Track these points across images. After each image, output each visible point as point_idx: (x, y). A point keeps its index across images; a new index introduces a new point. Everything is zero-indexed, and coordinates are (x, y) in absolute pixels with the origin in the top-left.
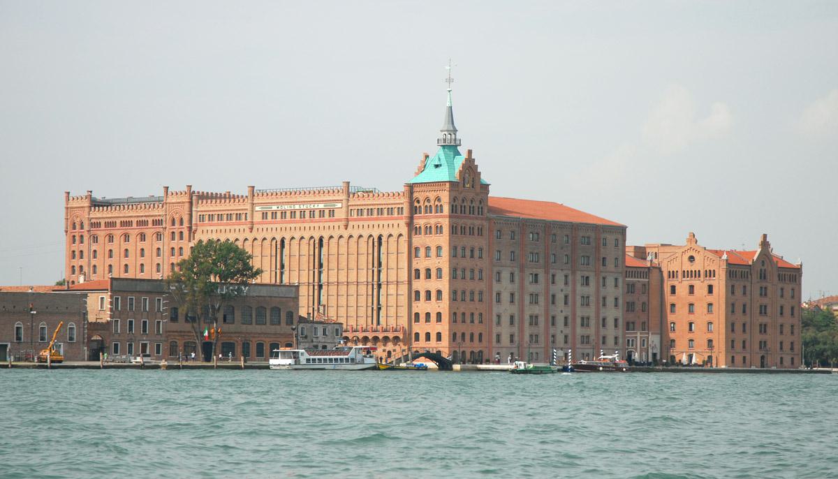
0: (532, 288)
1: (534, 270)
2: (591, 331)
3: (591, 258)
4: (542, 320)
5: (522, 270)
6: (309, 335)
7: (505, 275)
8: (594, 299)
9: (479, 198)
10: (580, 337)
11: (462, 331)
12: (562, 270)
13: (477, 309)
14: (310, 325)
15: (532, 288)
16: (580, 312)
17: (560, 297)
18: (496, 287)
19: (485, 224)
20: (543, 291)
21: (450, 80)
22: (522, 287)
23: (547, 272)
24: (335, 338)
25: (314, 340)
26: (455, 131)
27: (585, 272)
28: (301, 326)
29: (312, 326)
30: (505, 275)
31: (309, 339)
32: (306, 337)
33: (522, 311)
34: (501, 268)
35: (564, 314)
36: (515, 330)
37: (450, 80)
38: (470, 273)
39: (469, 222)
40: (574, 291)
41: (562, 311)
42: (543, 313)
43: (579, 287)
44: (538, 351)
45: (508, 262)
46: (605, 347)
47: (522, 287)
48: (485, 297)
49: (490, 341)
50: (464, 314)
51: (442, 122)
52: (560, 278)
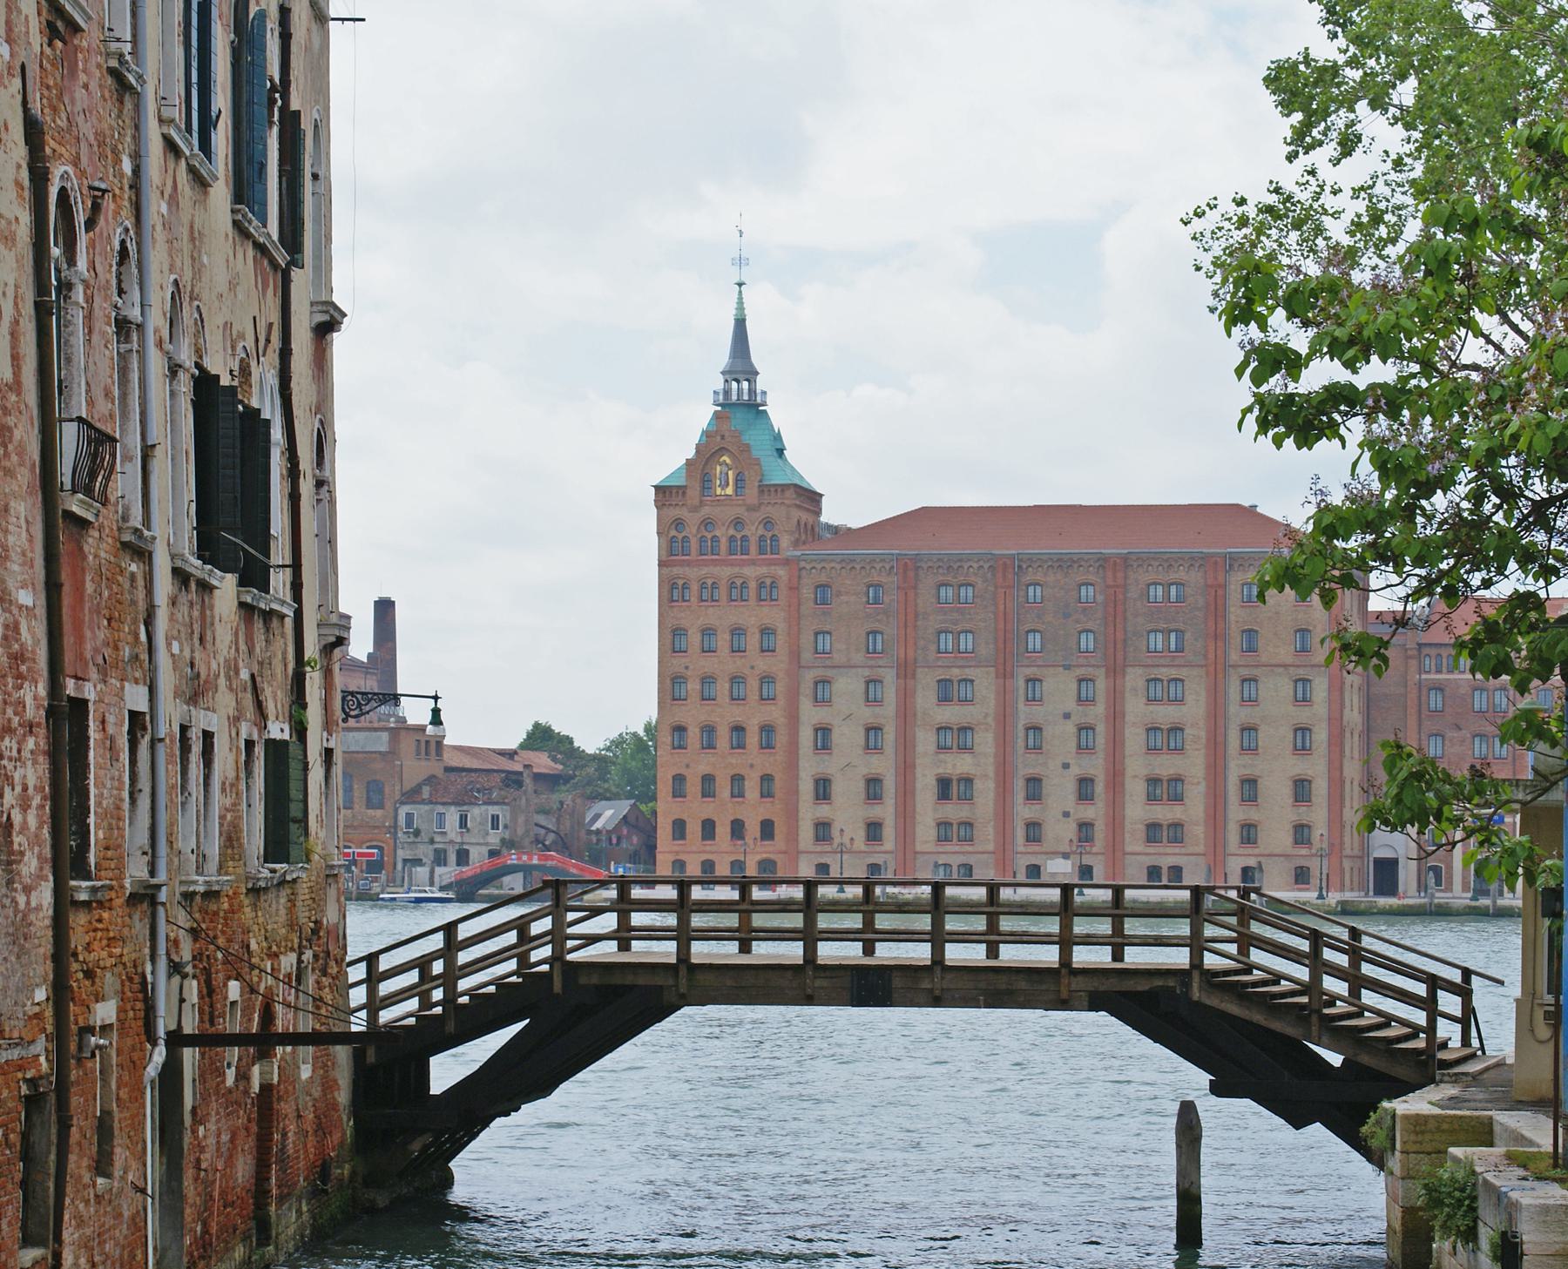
0: (951, 714)
1: (956, 671)
2: (1194, 809)
3: (1188, 636)
4: (985, 790)
5: (906, 671)
6: (423, 827)
7: (847, 687)
8: (1203, 734)
9: (760, 515)
10: (1142, 827)
11: (705, 816)
12: (1067, 667)
13: (752, 766)
14: (427, 807)
15: (951, 714)
16: (1137, 766)
17: (1061, 737)
18: (810, 715)
19: (781, 572)
20: (990, 720)
21: (740, 262)
22: (906, 715)
23: (1005, 674)
24: (487, 834)
25: (438, 838)
26: (751, 374)
27: (1164, 670)
28: (403, 811)
29: (433, 811)
30: (847, 687)
31: (424, 837)
32: (417, 833)
33: (906, 769)
34: (830, 673)
35: (1075, 771)
36: (886, 812)
37: (740, 262)
38: (727, 685)
39: (725, 572)
40: (1116, 716)
41: (1066, 766)
42: (991, 771)
43: (1136, 709)
44: (971, 860)
45: (859, 658)
46: (1256, 851)
47: (906, 715)
48: (781, 739)
49: (793, 836)
50: (708, 780)
51: (722, 355)
52: (1060, 689)
